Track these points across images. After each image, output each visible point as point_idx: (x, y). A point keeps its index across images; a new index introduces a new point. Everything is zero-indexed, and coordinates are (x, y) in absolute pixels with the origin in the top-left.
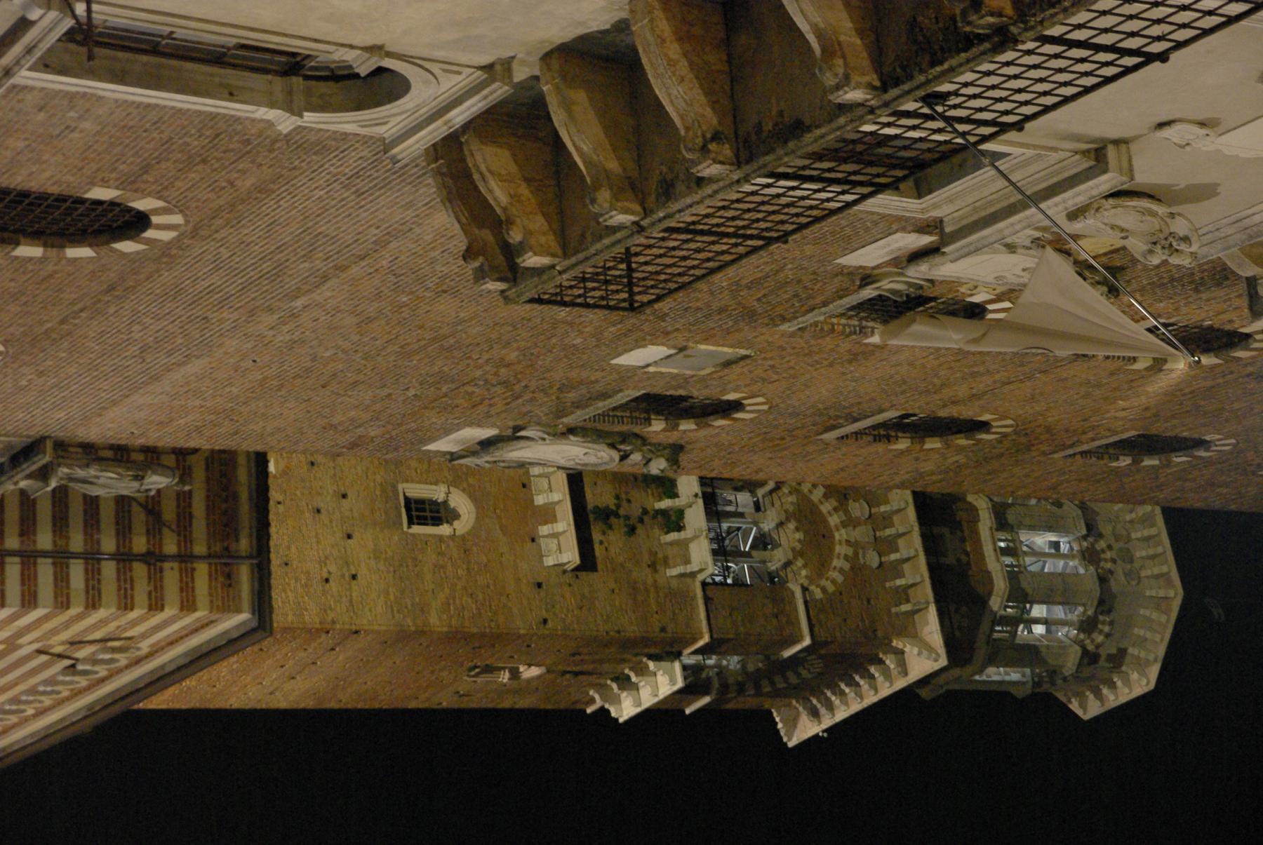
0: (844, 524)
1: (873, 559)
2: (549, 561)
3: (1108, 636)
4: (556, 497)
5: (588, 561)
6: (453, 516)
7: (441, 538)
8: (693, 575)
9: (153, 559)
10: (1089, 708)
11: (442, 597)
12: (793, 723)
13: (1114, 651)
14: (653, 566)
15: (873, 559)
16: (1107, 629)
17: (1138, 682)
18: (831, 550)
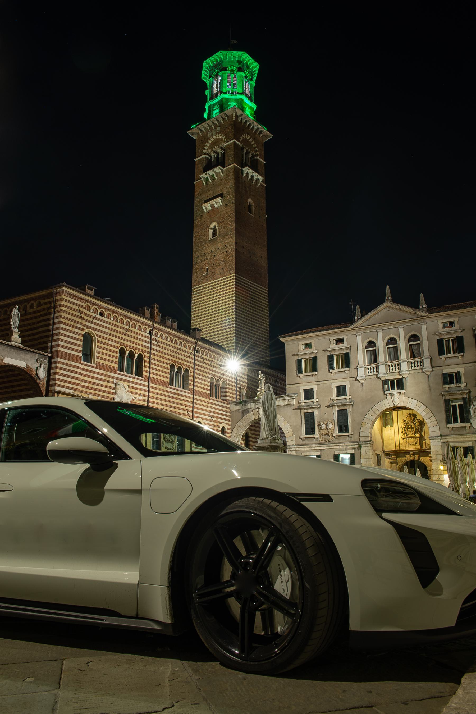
0: (213, 137)
1: (218, 128)
2: (221, 204)
3: (234, 66)
4: (209, 205)
5: (221, 195)
6: (215, 227)
7: (218, 229)
8: (222, 170)
9: (55, 307)
10: (255, 66)
11: (229, 226)
12: (266, 136)
13: (238, 64)
14: (222, 180)
15: (218, 128)
16: (232, 67)
17: (245, 56)
18: (218, 138)
